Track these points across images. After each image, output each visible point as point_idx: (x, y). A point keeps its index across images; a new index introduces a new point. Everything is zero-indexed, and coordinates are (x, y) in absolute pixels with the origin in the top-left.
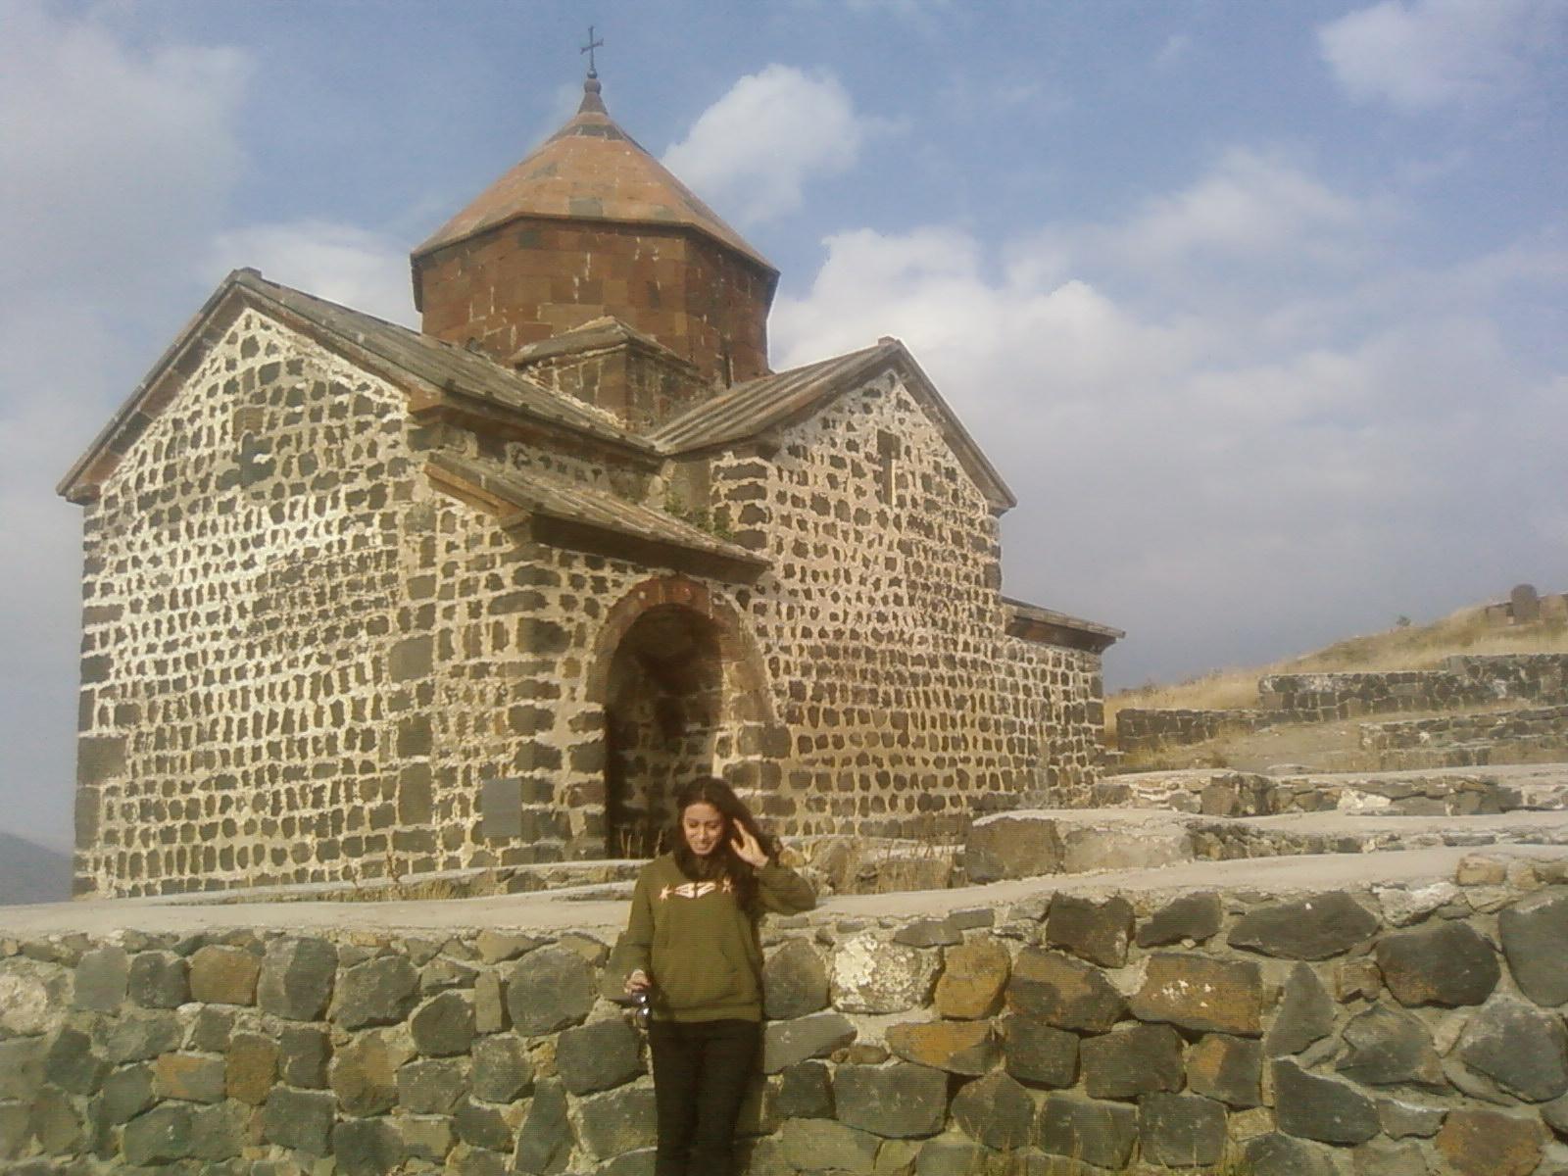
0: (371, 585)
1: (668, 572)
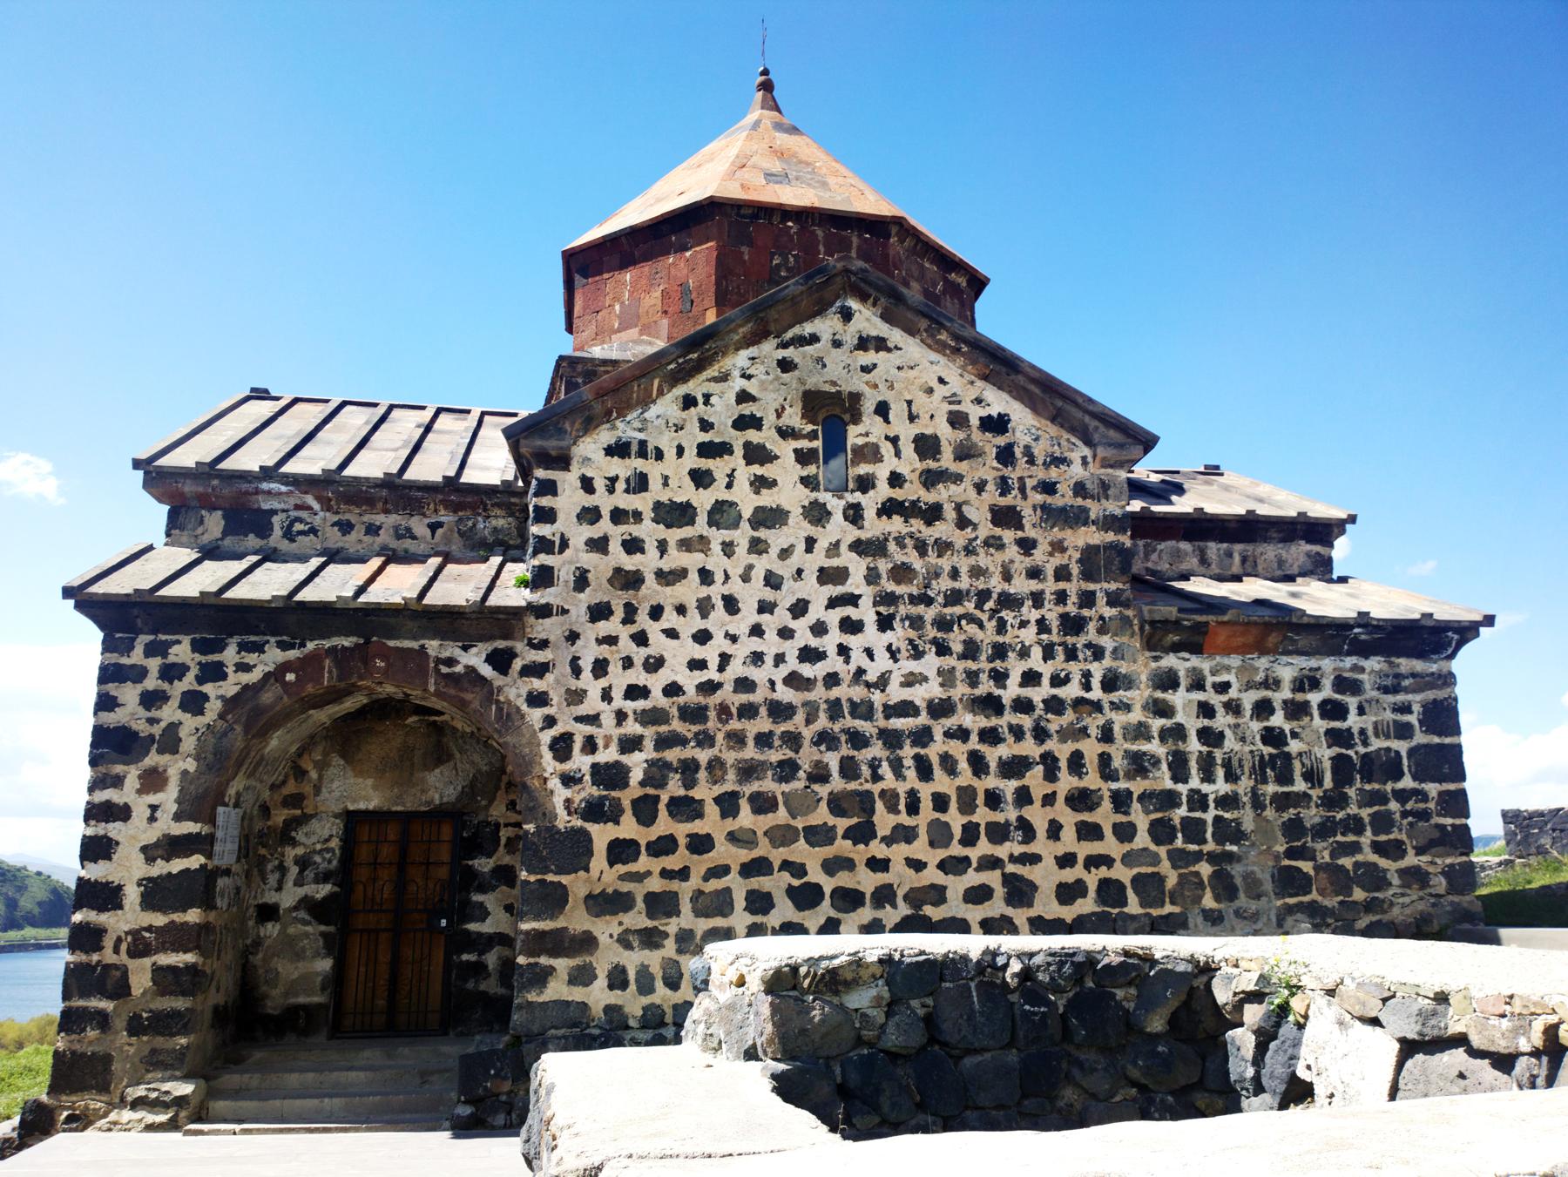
1: (347, 642)
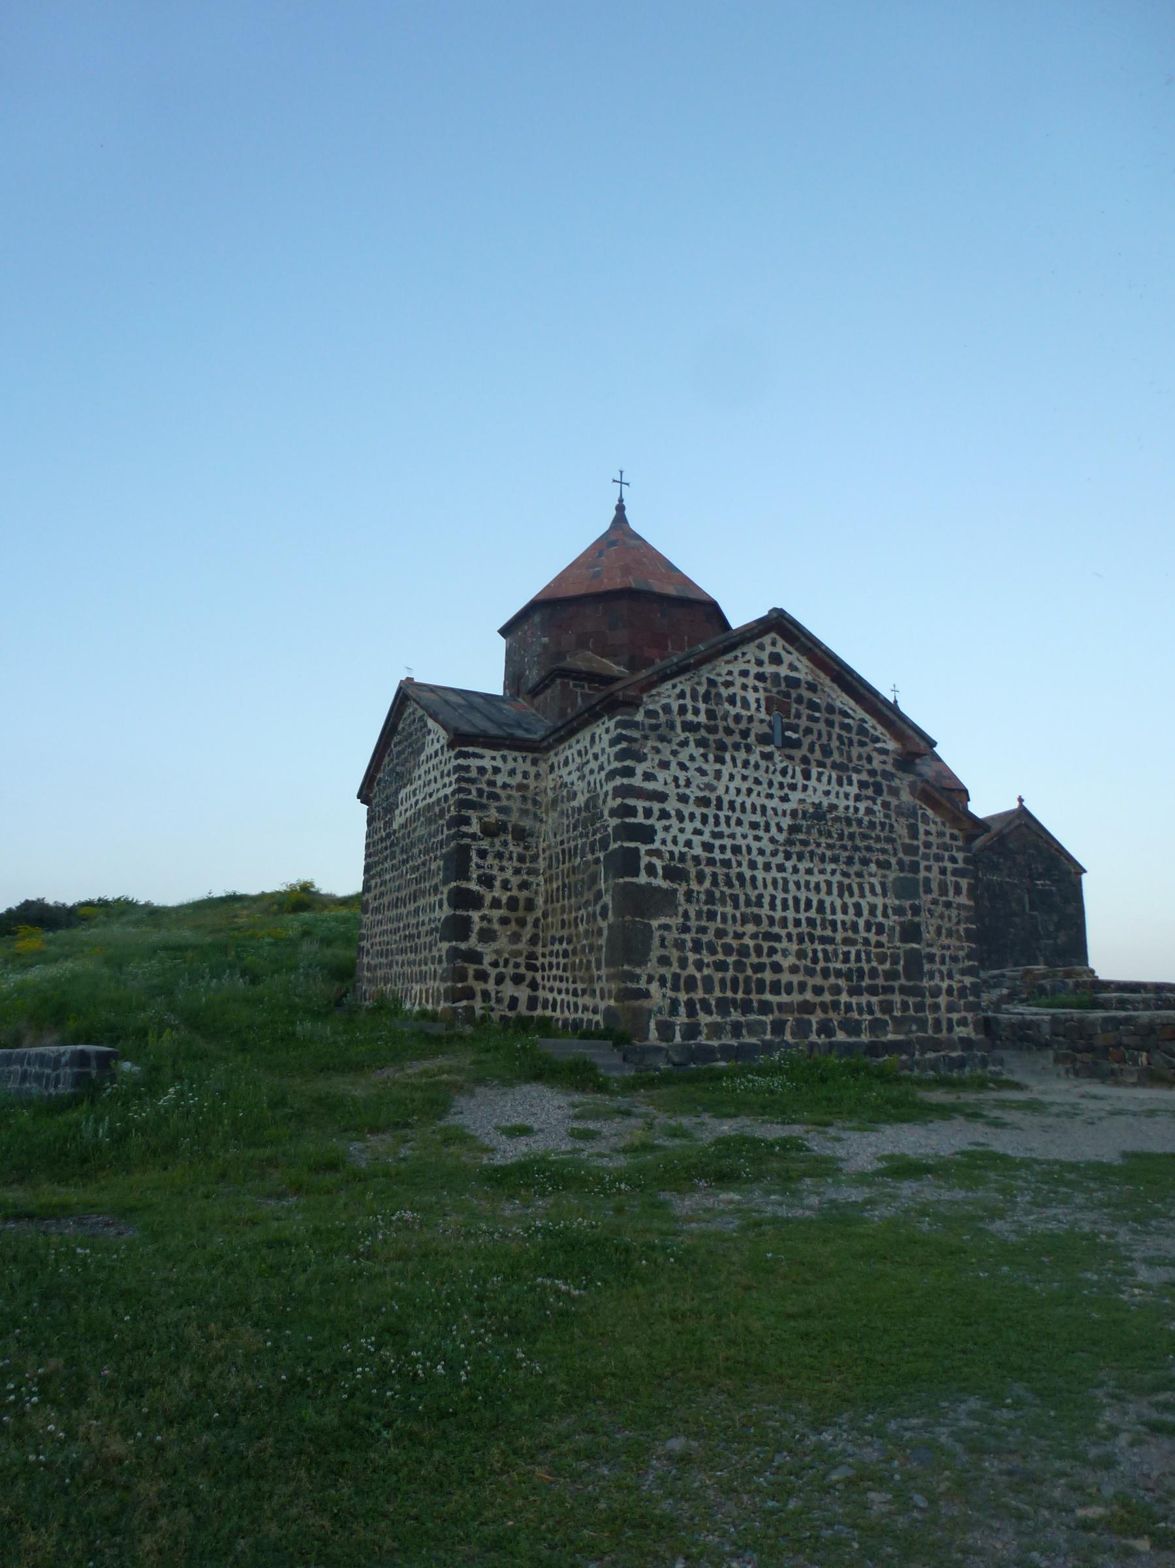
0: (878, 839)
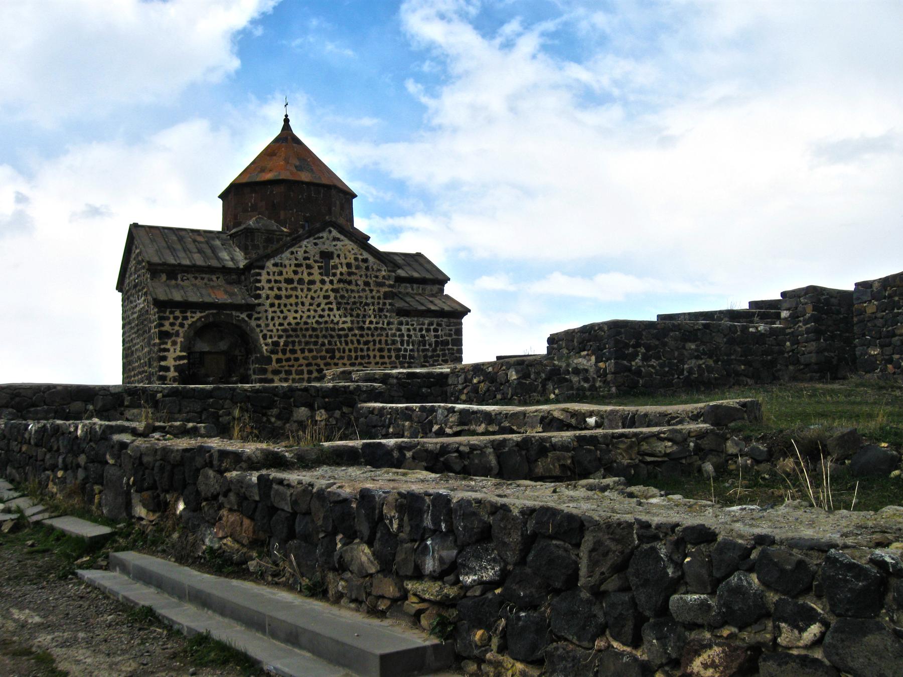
1: (215, 311)
